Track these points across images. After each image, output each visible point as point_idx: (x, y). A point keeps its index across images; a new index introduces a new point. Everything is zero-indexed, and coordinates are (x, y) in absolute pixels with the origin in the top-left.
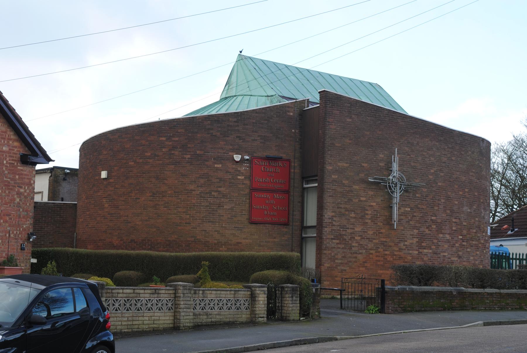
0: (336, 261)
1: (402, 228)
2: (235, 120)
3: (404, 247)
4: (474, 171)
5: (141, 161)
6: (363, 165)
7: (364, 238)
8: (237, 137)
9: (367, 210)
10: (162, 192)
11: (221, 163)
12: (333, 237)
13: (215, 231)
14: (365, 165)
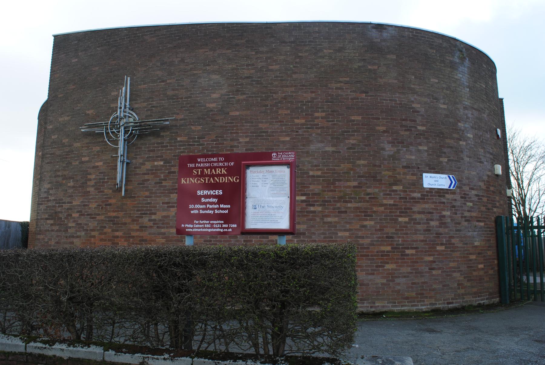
1: (147, 194)
3: (151, 224)
6: (87, 112)
7: (83, 215)
9: (90, 174)
12: (47, 217)
14: (90, 112)
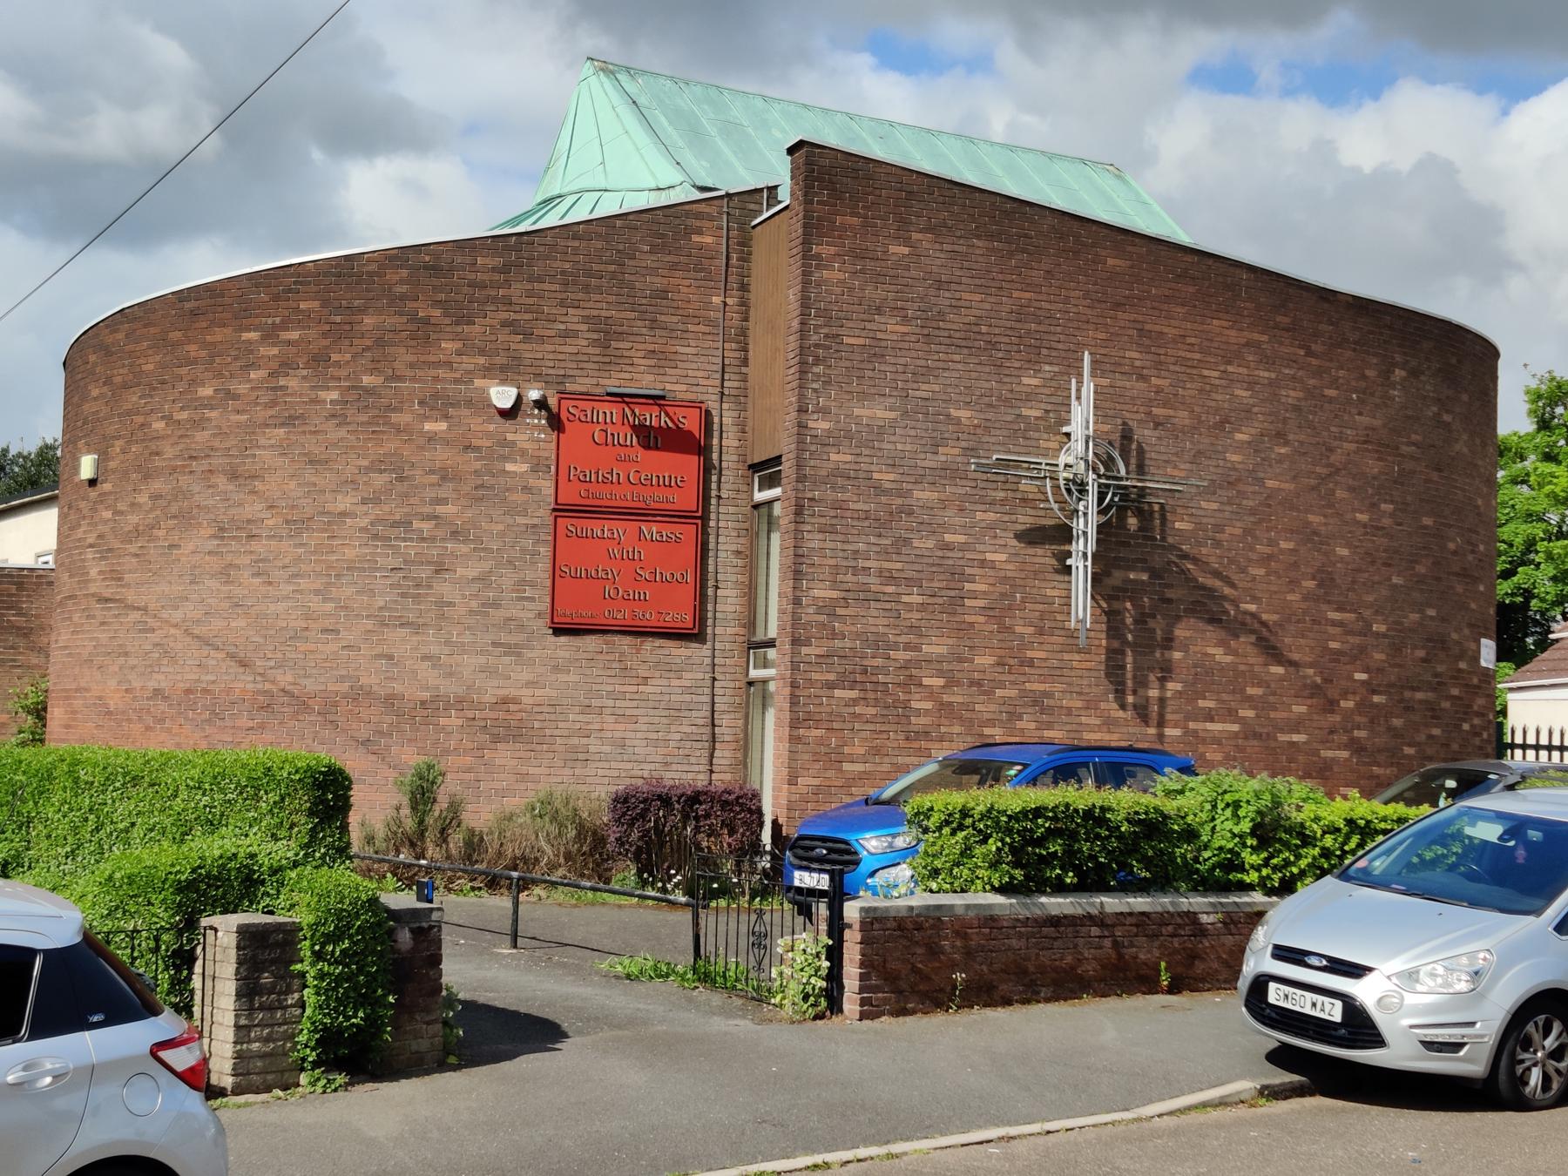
0: (846, 766)
2: (499, 261)
4: (1414, 437)
5: (184, 415)
8: (505, 324)
10: (249, 521)
11: (446, 417)
12: (832, 677)
13: (425, 658)
14: (963, 414)
